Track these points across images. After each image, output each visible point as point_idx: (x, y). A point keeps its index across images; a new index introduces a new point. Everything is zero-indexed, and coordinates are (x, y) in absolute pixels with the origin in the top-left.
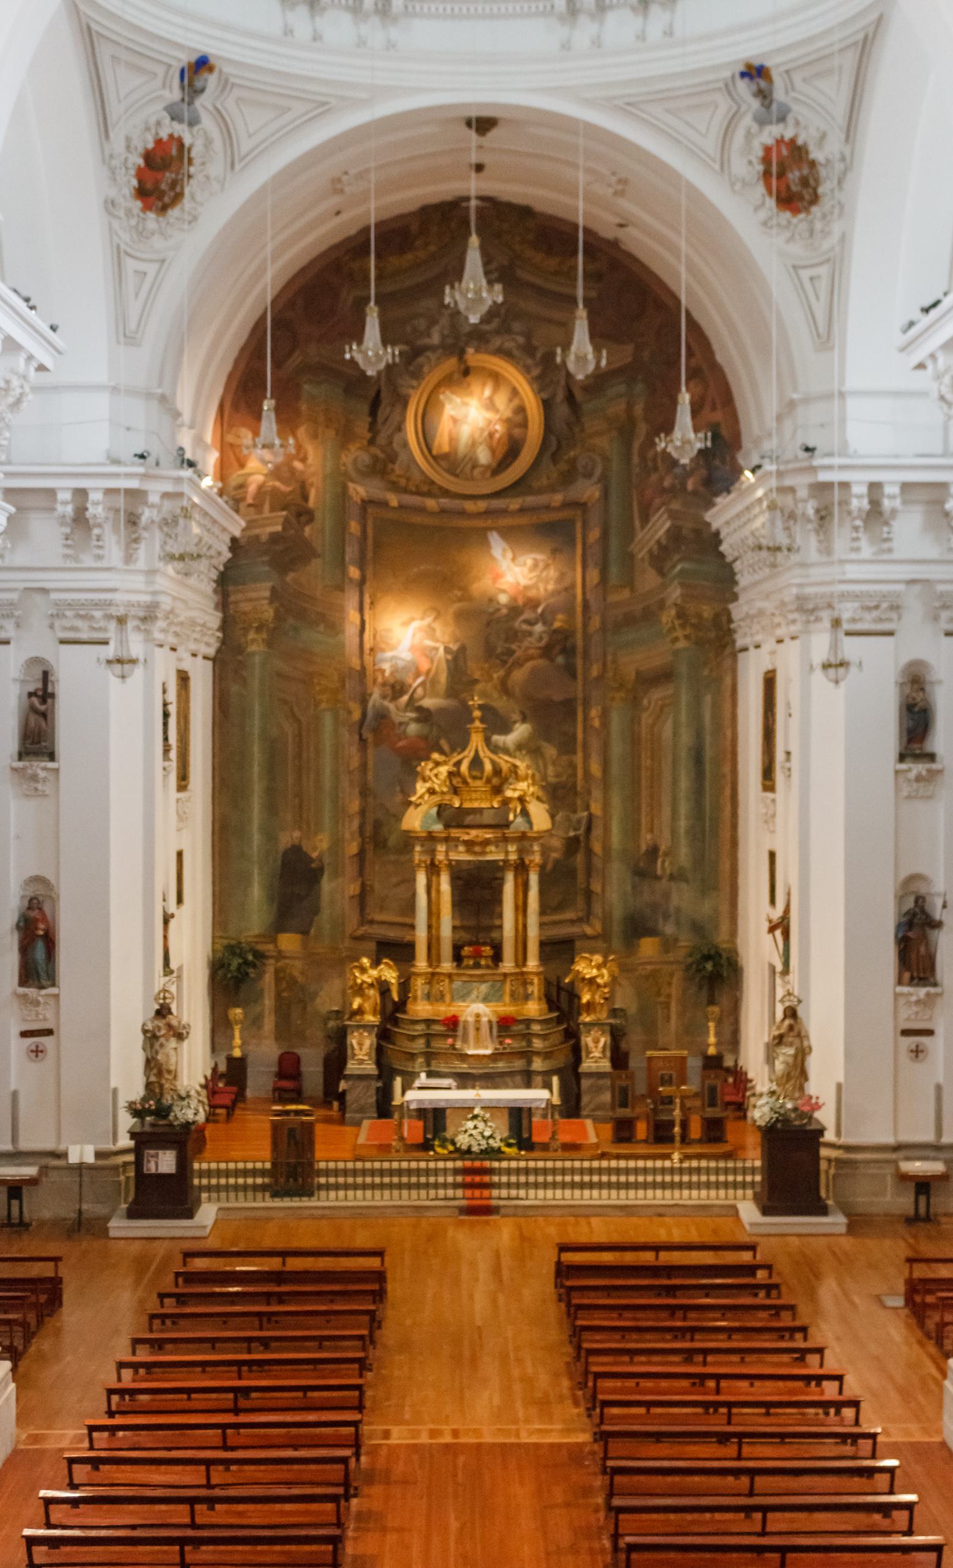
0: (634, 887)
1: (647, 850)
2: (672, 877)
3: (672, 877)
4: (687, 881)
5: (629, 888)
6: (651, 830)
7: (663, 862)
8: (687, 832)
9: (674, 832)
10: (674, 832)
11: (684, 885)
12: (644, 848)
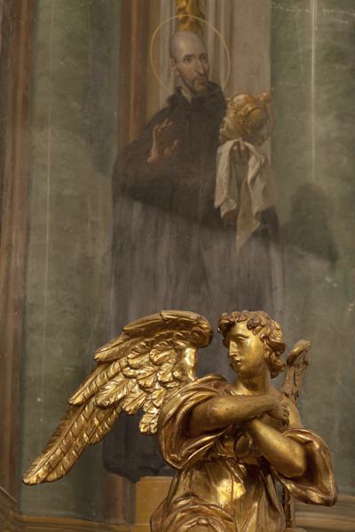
0: (121, 246)
1: (175, 100)
2: (269, 230)
3: (269, 230)
4: (332, 257)
5: (101, 249)
6: (198, 28)
7: (239, 158)
8: (333, 55)
9: (280, 48)
10: (280, 48)
11: (315, 265)
12: (163, 90)
